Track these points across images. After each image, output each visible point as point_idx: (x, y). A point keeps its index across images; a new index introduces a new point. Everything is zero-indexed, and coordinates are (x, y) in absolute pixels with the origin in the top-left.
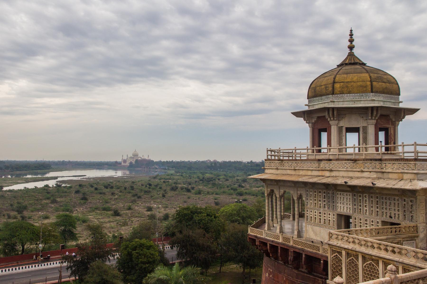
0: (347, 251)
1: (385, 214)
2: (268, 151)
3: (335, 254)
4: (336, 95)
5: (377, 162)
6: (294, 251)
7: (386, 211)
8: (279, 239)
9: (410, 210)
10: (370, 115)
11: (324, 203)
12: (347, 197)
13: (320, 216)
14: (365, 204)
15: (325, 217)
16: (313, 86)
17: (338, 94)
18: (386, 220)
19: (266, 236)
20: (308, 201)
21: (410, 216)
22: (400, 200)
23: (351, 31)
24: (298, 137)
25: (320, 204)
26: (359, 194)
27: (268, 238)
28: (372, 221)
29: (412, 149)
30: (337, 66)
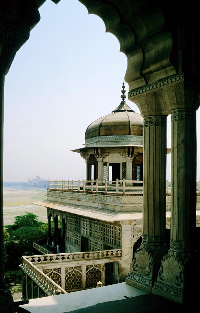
10: (127, 153)
17: (103, 136)
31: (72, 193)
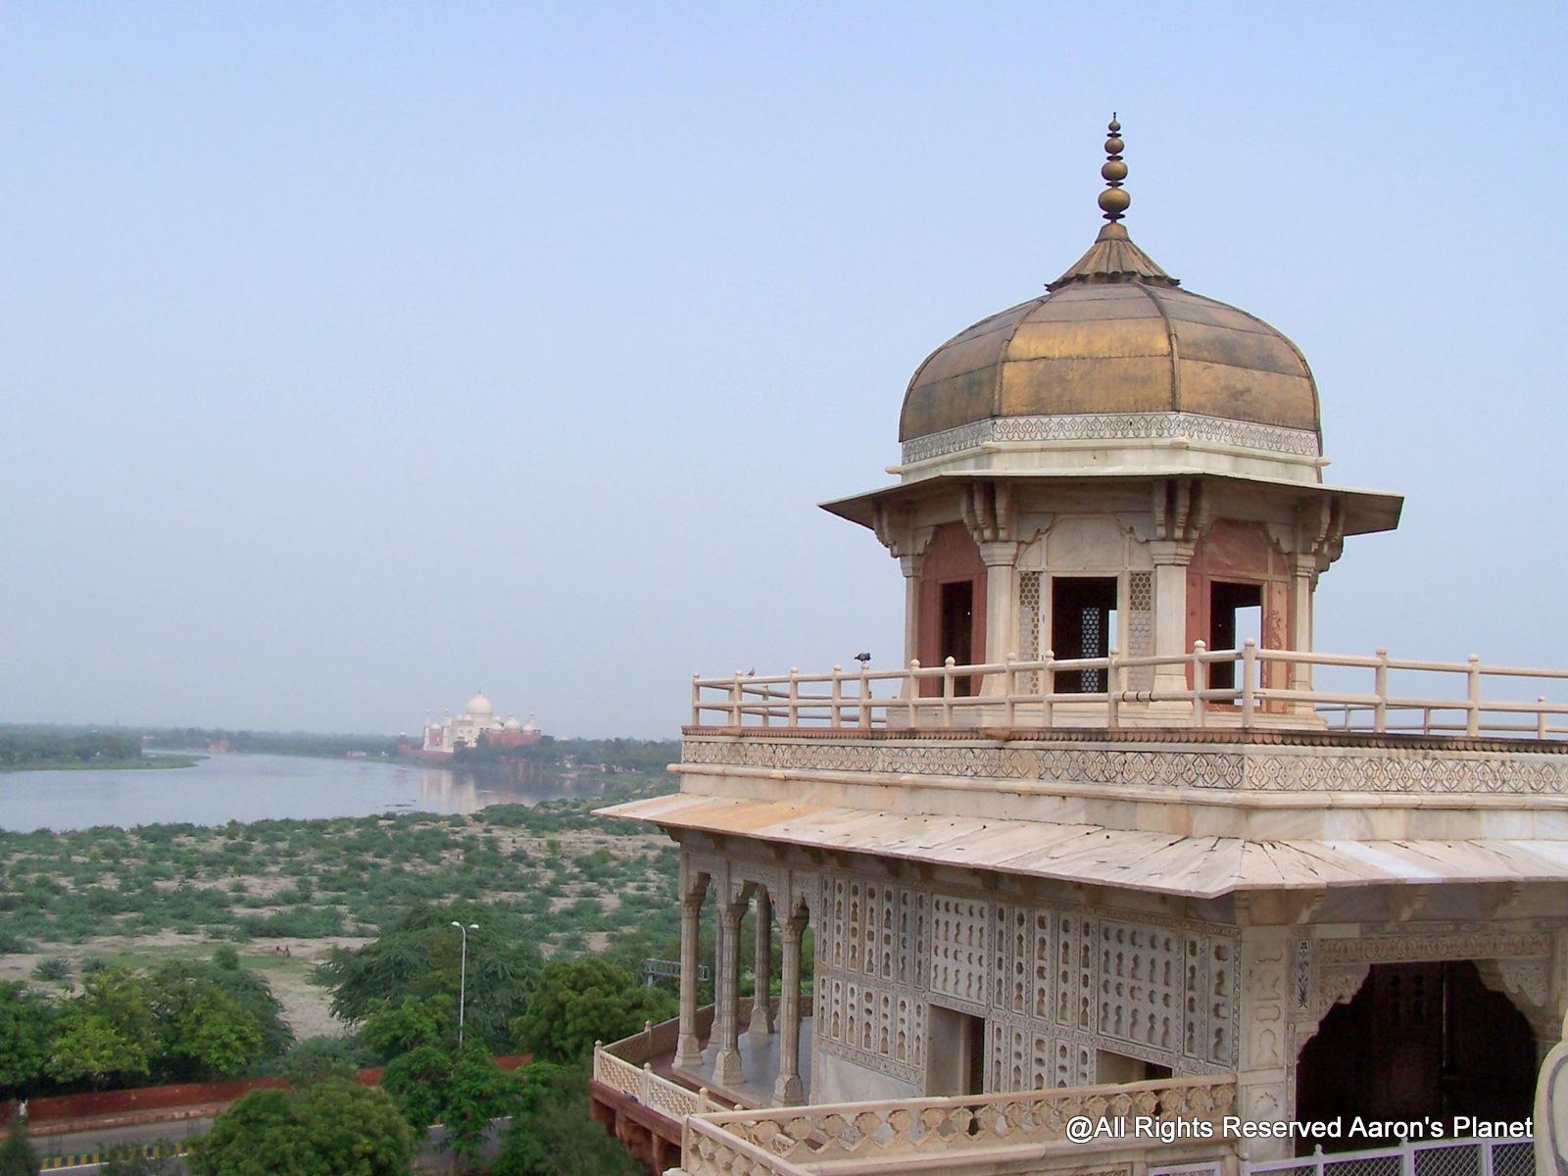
1: (1112, 1017)
4: (1010, 421)
9: (1215, 999)
11: (886, 949)
13: (869, 1012)
14: (1038, 963)
16: (922, 381)
17: (1021, 415)
18: (1114, 1049)
20: (825, 936)
21: (1213, 1029)
22: (1174, 946)
23: (1114, 130)
26: (1017, 911)
30: (1049, 288)
31: (868, 742)
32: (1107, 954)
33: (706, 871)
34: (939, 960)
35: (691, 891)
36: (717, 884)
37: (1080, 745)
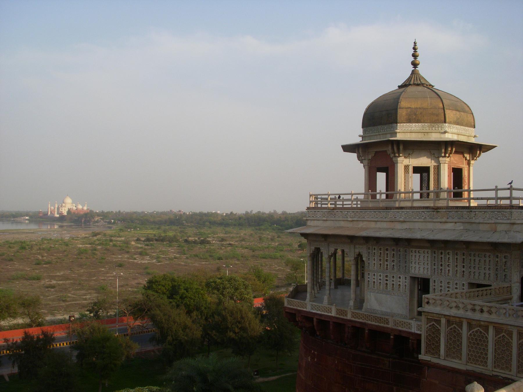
0: (448, 318)
1: (472, 274)
2: (311, 196)
3: (431, 324)
4: (402, 124)
5: (464, 210)
6: (352, 326)
7: (474, 271)
8: (331, 312)
10: (443, 151)
12: (424, 255)
13: (387, 280)
15: (393, 281)
19: (312, 309)
22: (492, 257)
24: (349, 177)
25: (387, 265)
26: (440, 251)
27: (313, 311)
28: (456, 284)
29: (507, 194)
30: (399, 87)
32: (470, 260)
33: (318, 247)
34: (414, 265)
35: (312, 252)
36: (323, 250)
37: (461, 210)
